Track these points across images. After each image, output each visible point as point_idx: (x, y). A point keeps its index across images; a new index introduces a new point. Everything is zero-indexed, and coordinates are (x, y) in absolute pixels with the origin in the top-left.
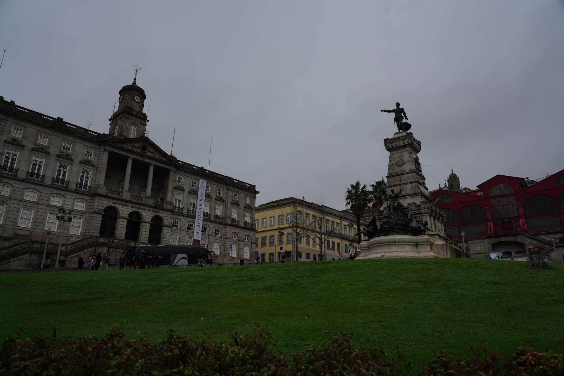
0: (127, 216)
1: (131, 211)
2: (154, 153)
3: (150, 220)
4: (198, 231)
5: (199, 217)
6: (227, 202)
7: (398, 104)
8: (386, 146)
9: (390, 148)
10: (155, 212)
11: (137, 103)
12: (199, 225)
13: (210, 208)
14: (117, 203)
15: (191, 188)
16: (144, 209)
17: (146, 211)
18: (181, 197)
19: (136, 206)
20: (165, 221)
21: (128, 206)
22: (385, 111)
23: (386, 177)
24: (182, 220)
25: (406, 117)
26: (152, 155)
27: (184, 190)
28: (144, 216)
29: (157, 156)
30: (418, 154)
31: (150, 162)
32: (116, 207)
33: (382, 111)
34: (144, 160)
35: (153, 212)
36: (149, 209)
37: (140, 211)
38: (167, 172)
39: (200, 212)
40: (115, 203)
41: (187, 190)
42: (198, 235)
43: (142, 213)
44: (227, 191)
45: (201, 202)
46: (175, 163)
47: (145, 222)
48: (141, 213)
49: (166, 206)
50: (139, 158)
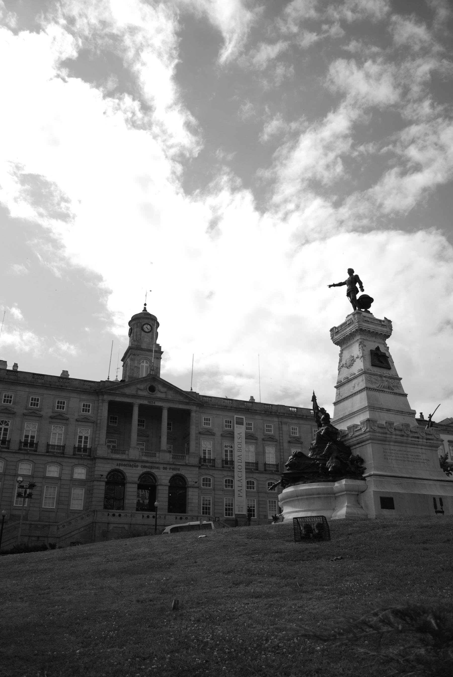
0: (136, 479)
1: (141, 472)
2: (165, 392)
3: (168, 481)
4: (240, 488)
5: (240, 467)
6: (281, 441)
7: (351, 271)
8: (333, 339)
9: (337, 341)
10: (173, 469)
11: (146, 334)
12: (240, 479)
13: (257, 454)
14: (122, 465)
16: (158, 468)
17: (162, 470)
18: (210, 444)
19: (147, 465)
20: (189, 480)
21: (137, 466)
22: (334, 285)
23: (335, 387)
24: (215, 476)
25: (361, 287)
26: (163, 396)
27: (213, 434)
28: (159, 477)
29: (171, 395)
30: (388, 341)
31: (162, 405)
32: (122, 469)
33: (330, 286)
34: (154, 404)
35: (171, 470)
36: (165, 466)
37: (153, 471)
38: (187, 413)
39: (240, 461)
40: (120, 465)
41: (218, 433)
42: (239, 493)
43: (156, 474)
44: (280, 426)
45: (239, 446)
47: (161, 485)
48: (155, 473)
49: (189, 460)
50: (146, 402)
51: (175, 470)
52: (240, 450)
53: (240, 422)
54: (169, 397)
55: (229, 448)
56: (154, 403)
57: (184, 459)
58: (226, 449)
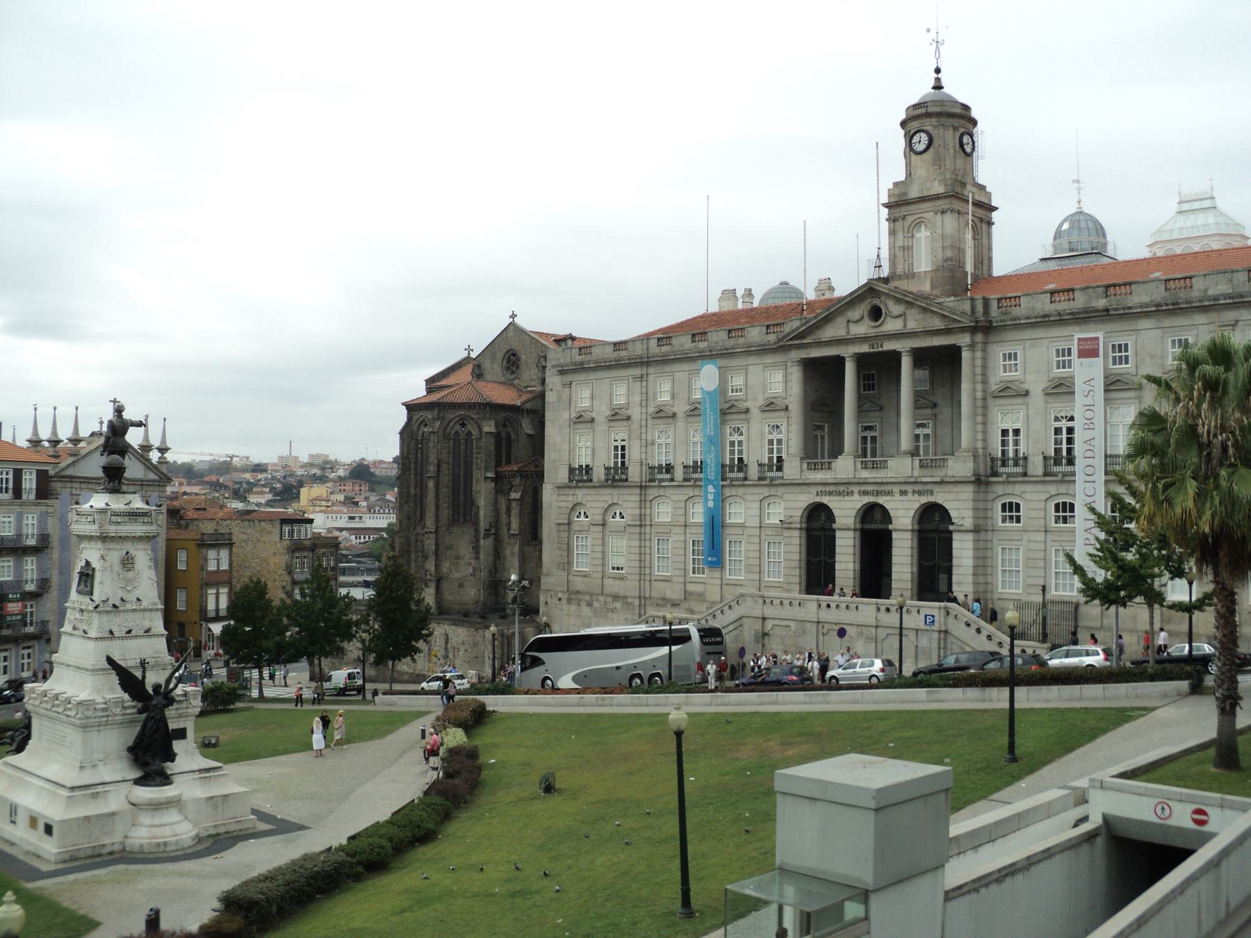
10: (920, 493)
15: (1052, 375)
16: (890, 493)
17: (897, 496)
19: (869, 488)
21: (852, 493)
36: (904, 488)
37: (881, 500)
45: (1089, 415)
46: (958, 321)
47: (896, 530)
50: (865, 348)
51: (924, 495)
52: (1091, 426)
53: (1088, 351)
54: (912, 325)
55: (1064, 421)
56: (882, 346)
57: (943, 466)
58: (1058, 424)
